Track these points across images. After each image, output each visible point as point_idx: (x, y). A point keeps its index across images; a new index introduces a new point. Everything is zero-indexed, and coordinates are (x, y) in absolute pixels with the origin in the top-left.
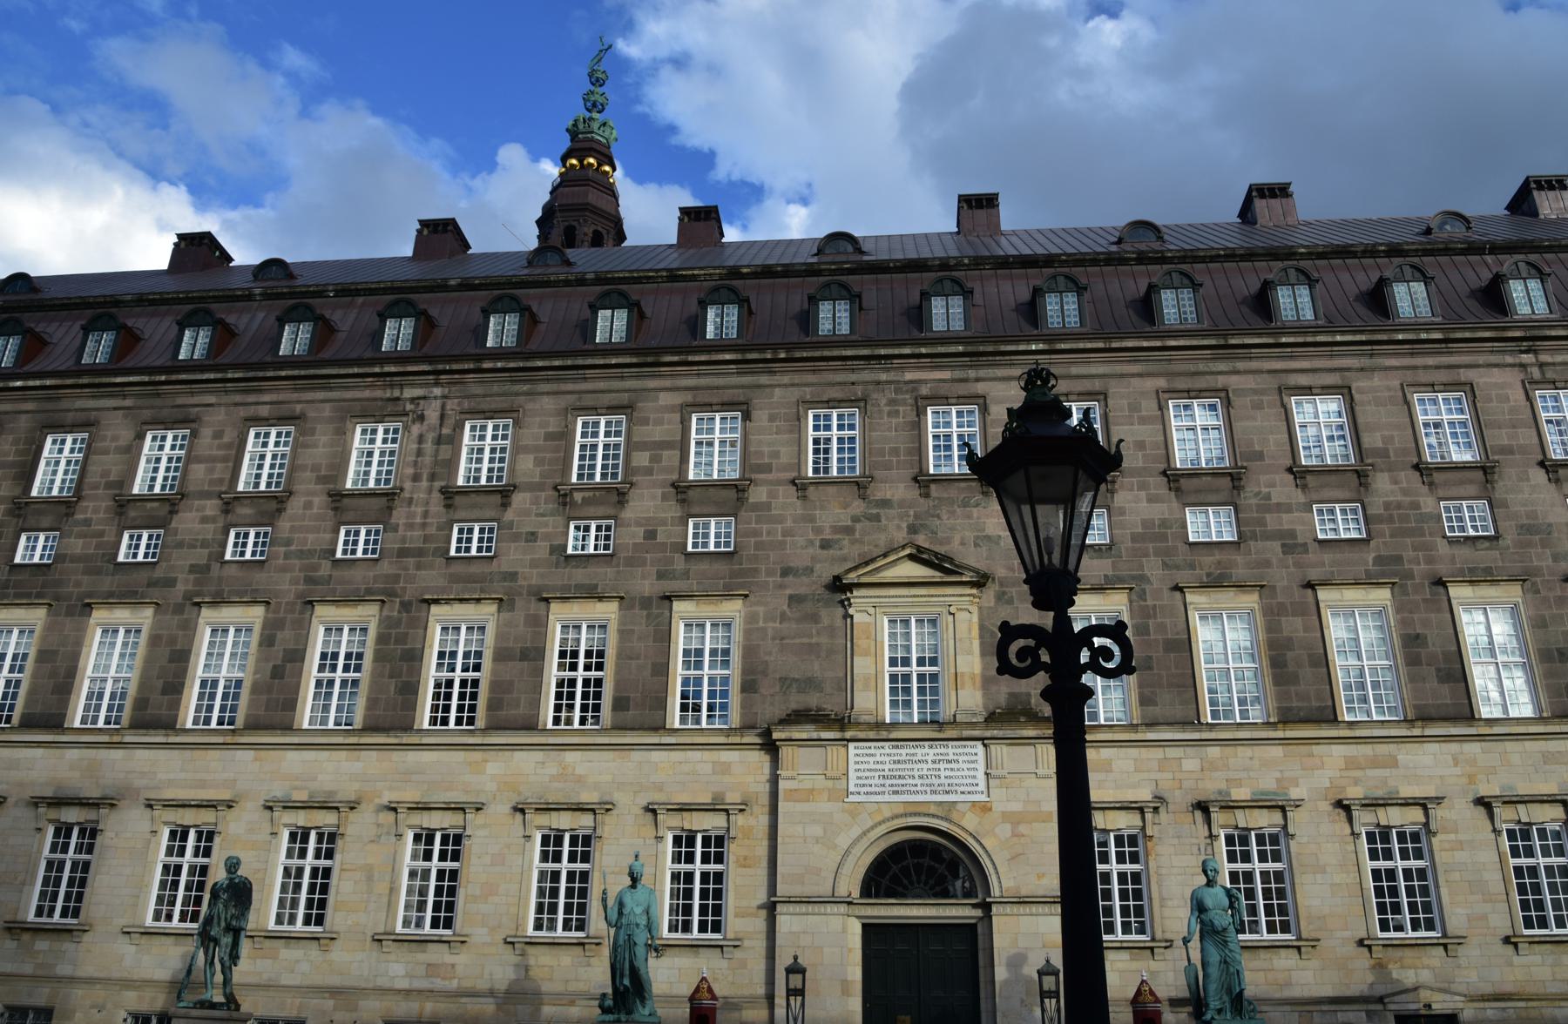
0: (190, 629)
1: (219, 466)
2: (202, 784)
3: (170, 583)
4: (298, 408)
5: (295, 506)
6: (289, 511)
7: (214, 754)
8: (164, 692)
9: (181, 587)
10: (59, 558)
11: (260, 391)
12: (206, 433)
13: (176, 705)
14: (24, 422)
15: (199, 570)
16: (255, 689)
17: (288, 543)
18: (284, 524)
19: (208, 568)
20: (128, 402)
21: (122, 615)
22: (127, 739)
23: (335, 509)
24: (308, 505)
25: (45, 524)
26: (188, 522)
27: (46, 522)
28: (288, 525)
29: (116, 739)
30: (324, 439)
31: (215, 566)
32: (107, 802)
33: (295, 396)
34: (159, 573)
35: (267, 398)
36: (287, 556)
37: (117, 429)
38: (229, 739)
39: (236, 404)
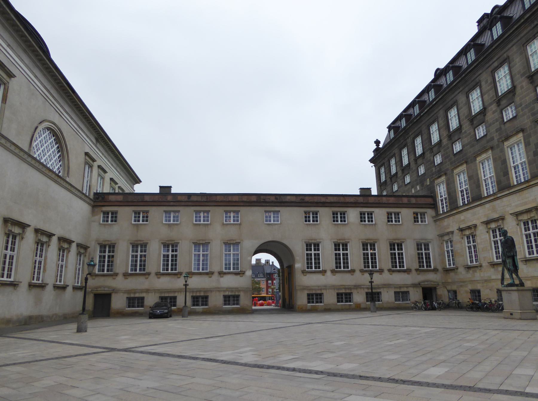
0: (503, 151)
1: (491, 92)
2: (526, 203)
3: (492, 139)
4: (505, 55)
5: (518, 91)
6: (517, 93)
7: (525, 192)
8: (504, 176)
9: (496, 138)
10: (463, 147)
11: (492, 58)
12: (483, 83)
13: (508, 179)
14: (441, 113)
15: (499, 130)
16: (530, 163)
17: (521, 105)
18: (517, 99)
19: (500, 128)
20: (461, 89)
21: (484, 156)
22: (499, 195)
23: (531, 83)
24: (522, 87)
25: (456, 139)
26: (490, 116)
27: (456, 138)
28: (518, 98)
29: (496, 197)
30: (517, 60)
31: (502, 126)
32: (502, 219)
33: (503, 52)
34: (488, 137)
35: (495, 59)
36: (522, 110)
37: (462, 99)
38: (527, 185)
39: (487, 68)
